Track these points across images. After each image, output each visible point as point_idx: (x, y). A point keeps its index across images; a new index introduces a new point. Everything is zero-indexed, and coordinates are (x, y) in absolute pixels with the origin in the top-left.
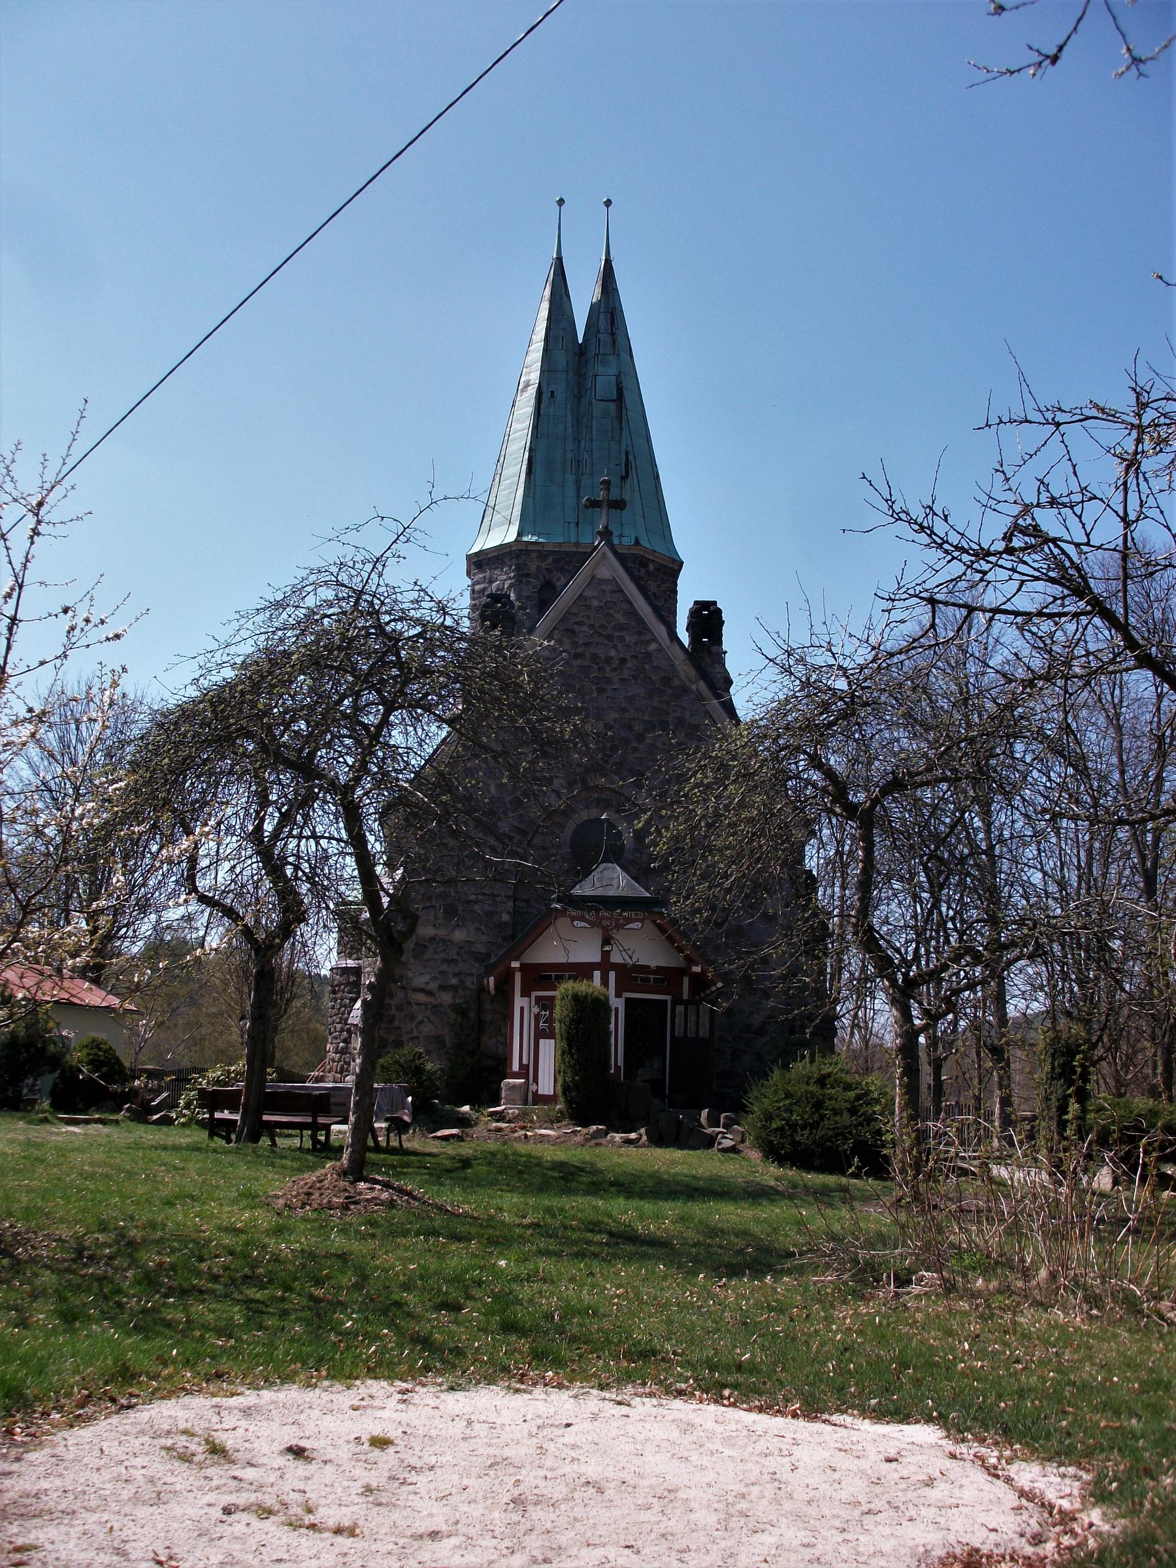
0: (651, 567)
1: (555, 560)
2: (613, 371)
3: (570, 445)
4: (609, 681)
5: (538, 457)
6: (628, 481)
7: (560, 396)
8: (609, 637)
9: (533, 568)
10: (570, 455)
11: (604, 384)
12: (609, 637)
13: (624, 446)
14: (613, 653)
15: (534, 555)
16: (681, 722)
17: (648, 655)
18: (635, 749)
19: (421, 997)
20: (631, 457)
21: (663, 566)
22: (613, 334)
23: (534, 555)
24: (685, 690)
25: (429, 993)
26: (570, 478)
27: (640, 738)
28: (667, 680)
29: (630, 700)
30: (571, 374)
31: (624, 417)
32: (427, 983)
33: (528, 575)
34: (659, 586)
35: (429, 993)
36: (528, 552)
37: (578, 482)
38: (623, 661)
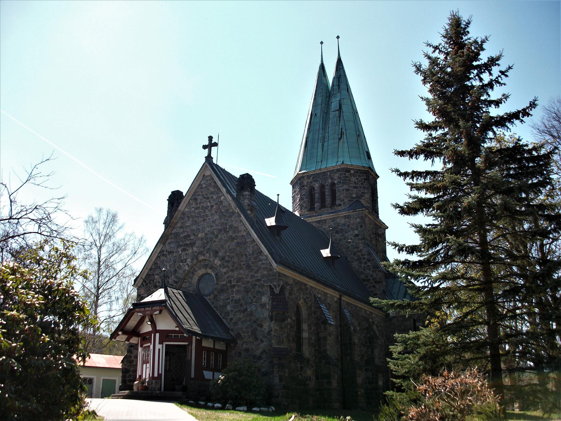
0: (352, 171)
1: (313, 178)
2: (338, 99)
3: (321, 132)
4: (207, 216)
5: (309, 139)
6: (341, 140)
7: (318, 114)
8: (208, 198)
9: (305, 183)
10: (320, 136)
11: (334, 105)
12: (208, 198)
13: (340, 127)
14: (209, 204)
15: (305, 178)
16: (231, 226)
17: (221, 202)
18: (215, 242)
20: (344, 130)
21: (359, 170)
22: (339, 85)
23: (305, 178)
24: (233, 213)
26: (320, 144)
27: (217, 236)
28: (227, 211)
29: (214, 222)
30: (324, 105)
31: (341, 115)
33: (304, 186)
34: (357, 179)
36: (303, 177)
37: (323, 145)
38: (212, 206)
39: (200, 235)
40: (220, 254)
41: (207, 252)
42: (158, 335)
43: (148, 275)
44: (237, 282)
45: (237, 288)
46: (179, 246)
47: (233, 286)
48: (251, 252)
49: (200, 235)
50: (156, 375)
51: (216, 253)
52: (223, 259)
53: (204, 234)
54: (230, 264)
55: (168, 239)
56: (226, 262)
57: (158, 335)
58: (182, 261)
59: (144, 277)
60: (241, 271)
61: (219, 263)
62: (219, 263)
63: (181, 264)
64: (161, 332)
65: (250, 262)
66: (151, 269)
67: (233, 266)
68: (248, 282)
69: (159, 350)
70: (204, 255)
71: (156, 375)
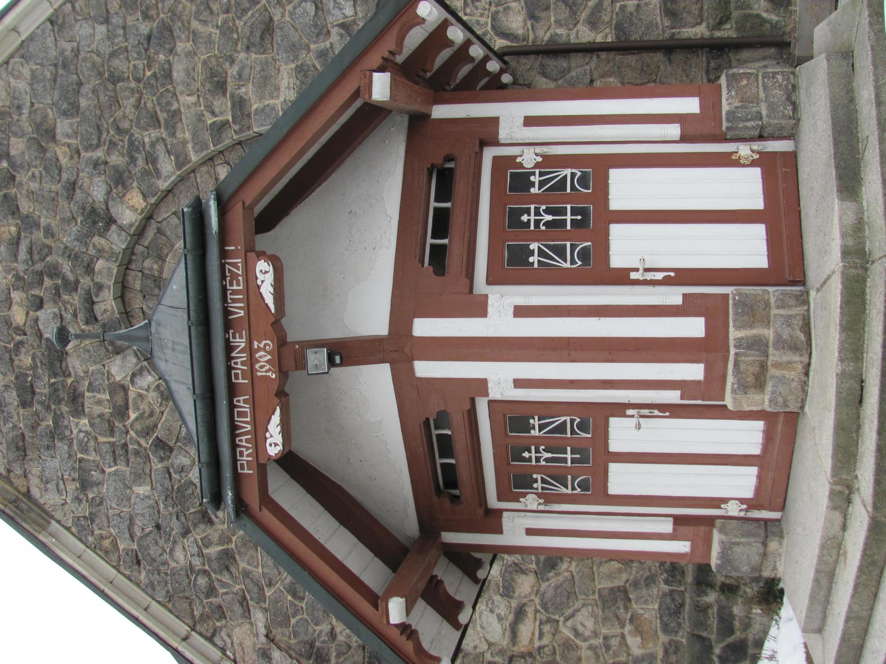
19: (526, 630)
25: (520, 614)
32: (500, 618)
35: (520, 614)
39: (19, 316)
40: (98, 190)
41: (89, 269)
42: (425, 327)
43: (169, 602)
44: (220, 86)
45: (248, 91)
46: (57, 433)
47: (240, 104)
48: (102, 29)
49: (19, 316)
50: (693, 327)
51: (100, 219)
52: (119, 180)
53: (16, 296)
54: (148, 137)
55: (28, 494)
56: (133, 160)
57: (425, 327)
58: (122, 412)
59: (184, 629)
60: (178, 73)
61: (136, 199)
62: (136, 199)
63: (133, 415)
64: (406, 304)
65: (144, 28)
66: (150, 588)
67: (155, 121)
68: (227, 30)
69: (521, 312)
70: (100, 287)
71: (693, 327)
